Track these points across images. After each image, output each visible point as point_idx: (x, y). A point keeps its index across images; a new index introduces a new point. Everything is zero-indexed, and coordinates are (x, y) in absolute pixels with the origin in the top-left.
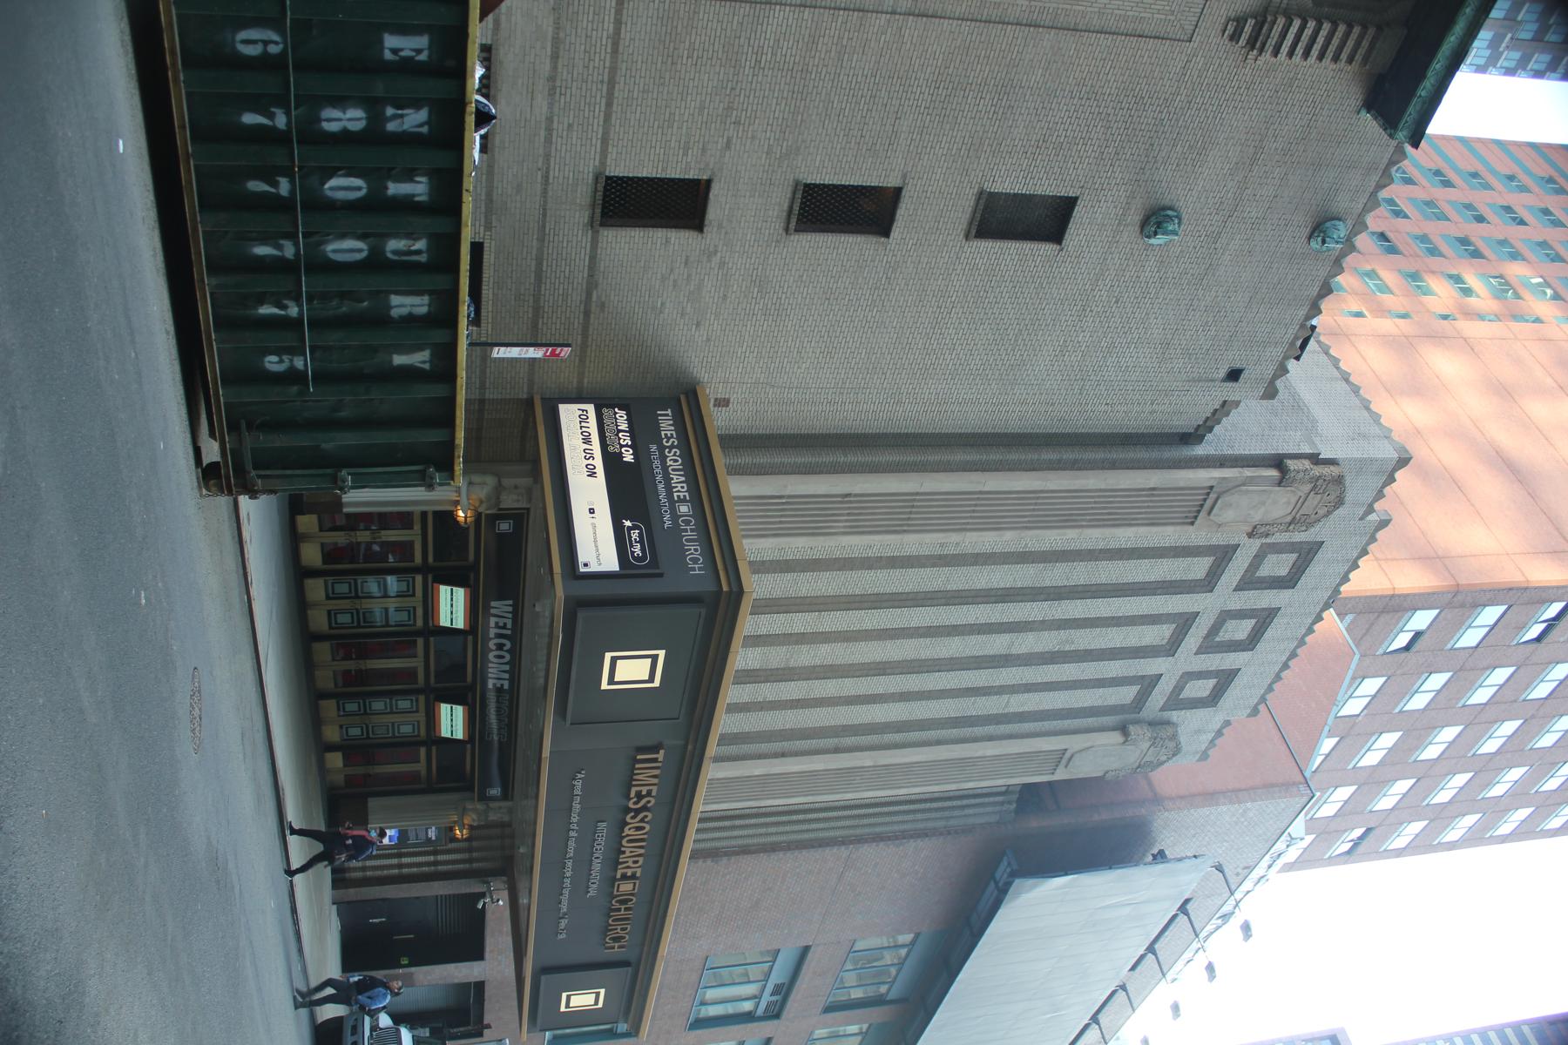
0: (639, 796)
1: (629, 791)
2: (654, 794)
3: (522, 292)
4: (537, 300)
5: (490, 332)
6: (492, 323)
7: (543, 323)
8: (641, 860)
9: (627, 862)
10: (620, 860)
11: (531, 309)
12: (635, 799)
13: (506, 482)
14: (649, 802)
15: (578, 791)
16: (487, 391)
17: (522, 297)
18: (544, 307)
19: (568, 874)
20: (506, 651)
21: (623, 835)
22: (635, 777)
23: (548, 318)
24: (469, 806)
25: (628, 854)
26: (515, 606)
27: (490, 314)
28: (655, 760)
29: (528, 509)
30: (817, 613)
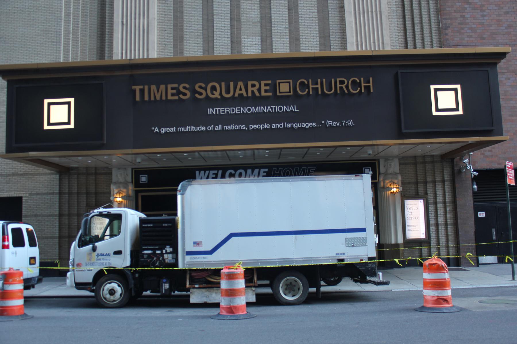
0: (179, 92)
1: (175, 101)
2: (176, 85)
3: (5, 181)
4: (9, 175)
5: (25, 192)
6: (20, 192)
7: (21, 172)
8: (250, 83)
9: (253, 92)
10: (250, 94)
11: (13, 177)
12: (181, 96)
13: (114, 179)
14: (185, 88)
15: (173, 130)
16: (55, 192)
17: (8, 181)
18: (13, 172)
19: (268, 126)
20: (236, 171)
21: (219, 97)
22: (158, 98)
23: (18, 170)
24: (382, 184)
25: (243, 92)
26: (200, 170)
27: (16, 193)
28: (142, 91)
29: (132, 169)
30: (214, 16)
